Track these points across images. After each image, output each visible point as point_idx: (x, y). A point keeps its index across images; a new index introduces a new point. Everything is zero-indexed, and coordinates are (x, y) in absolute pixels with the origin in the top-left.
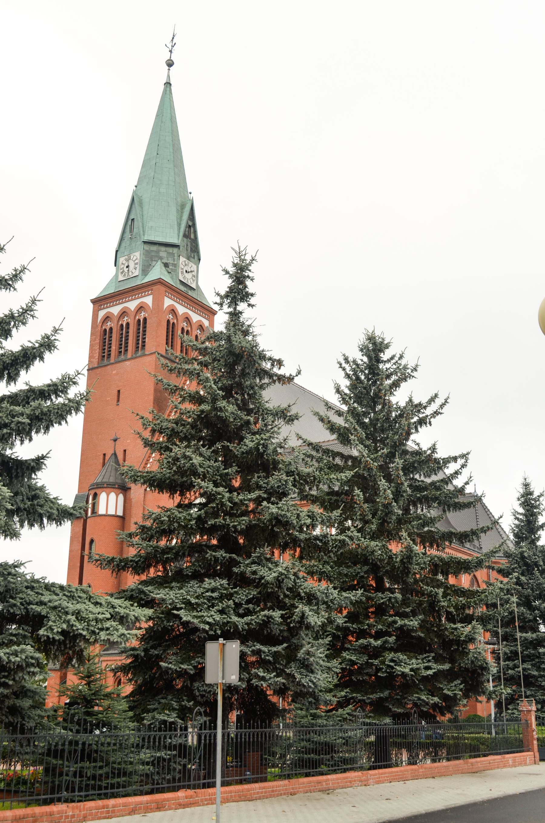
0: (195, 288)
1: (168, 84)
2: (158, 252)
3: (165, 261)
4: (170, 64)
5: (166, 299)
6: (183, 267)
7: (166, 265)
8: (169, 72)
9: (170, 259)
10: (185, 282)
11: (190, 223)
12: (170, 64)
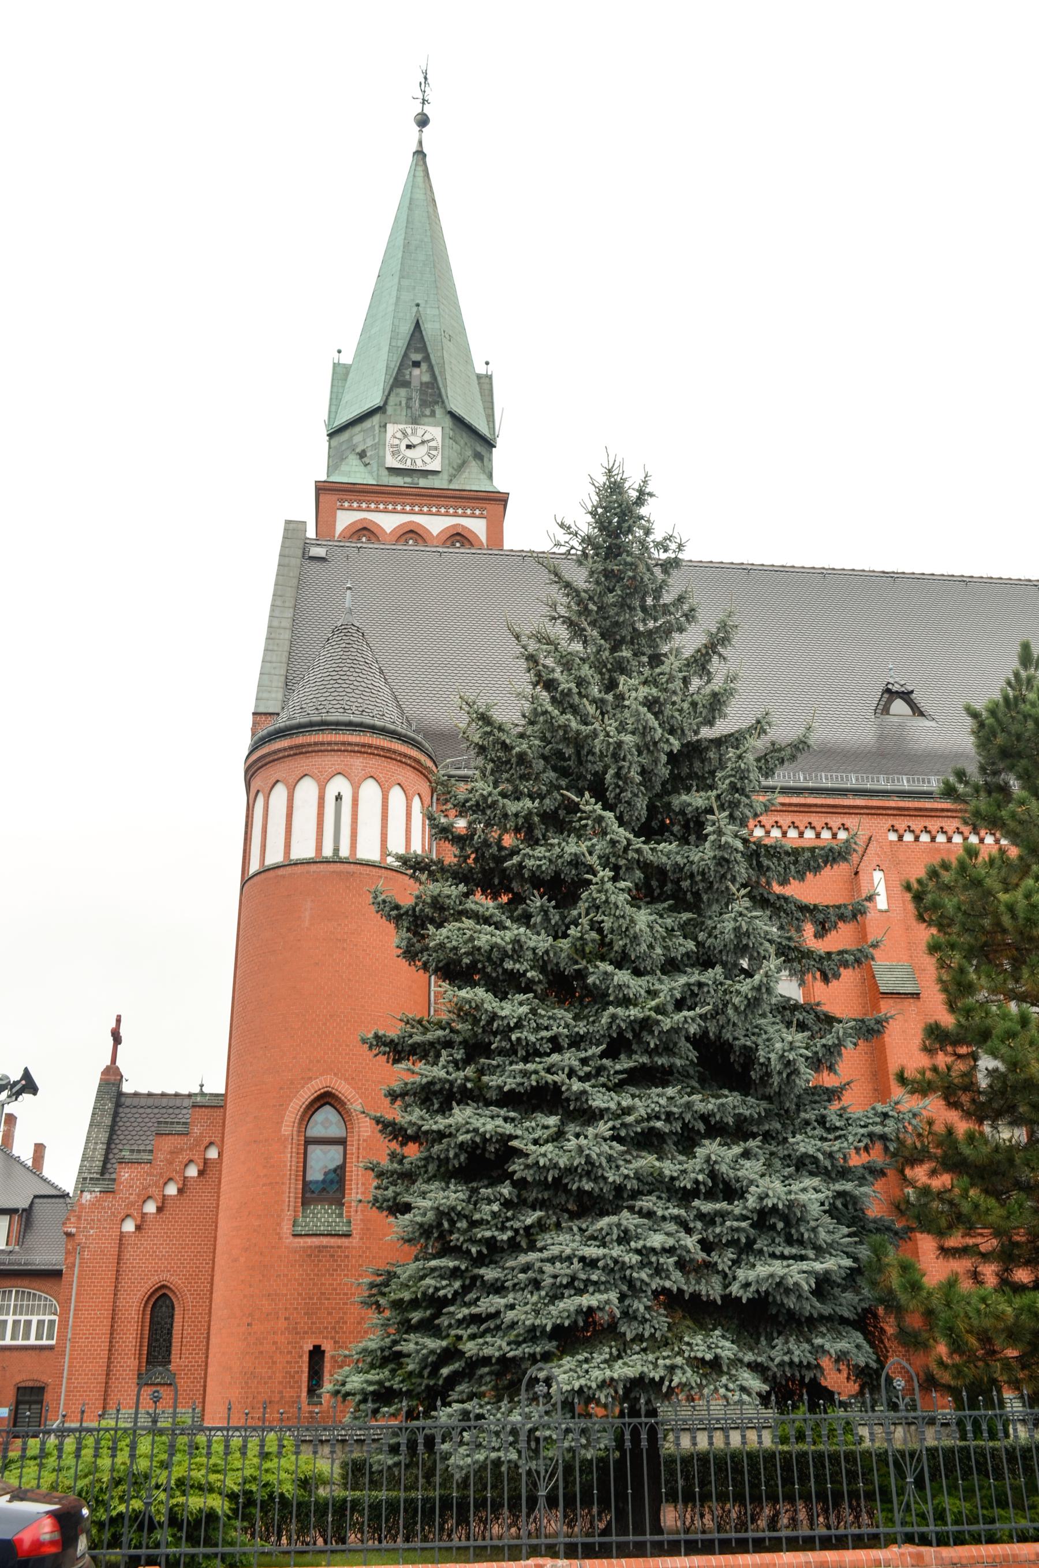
0: (439, 469)
1: (420, 154)
2: (351, 439)
3: (358, 450)
4: (423, 121)
5: (339, 513)
6: (397, 442)
7: (362, 455)
8: (420, 135)
9: (368, 440)
10: (408, 465)
11: (417, 357)
12: (423, 121)
